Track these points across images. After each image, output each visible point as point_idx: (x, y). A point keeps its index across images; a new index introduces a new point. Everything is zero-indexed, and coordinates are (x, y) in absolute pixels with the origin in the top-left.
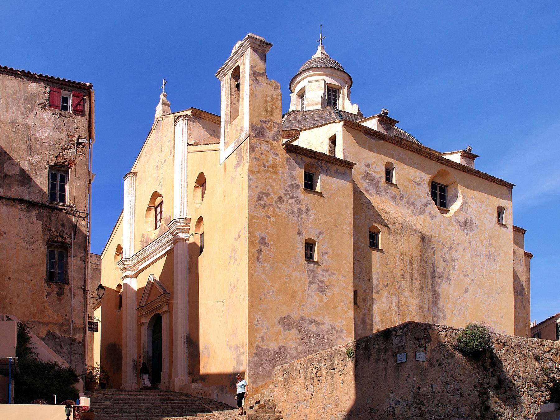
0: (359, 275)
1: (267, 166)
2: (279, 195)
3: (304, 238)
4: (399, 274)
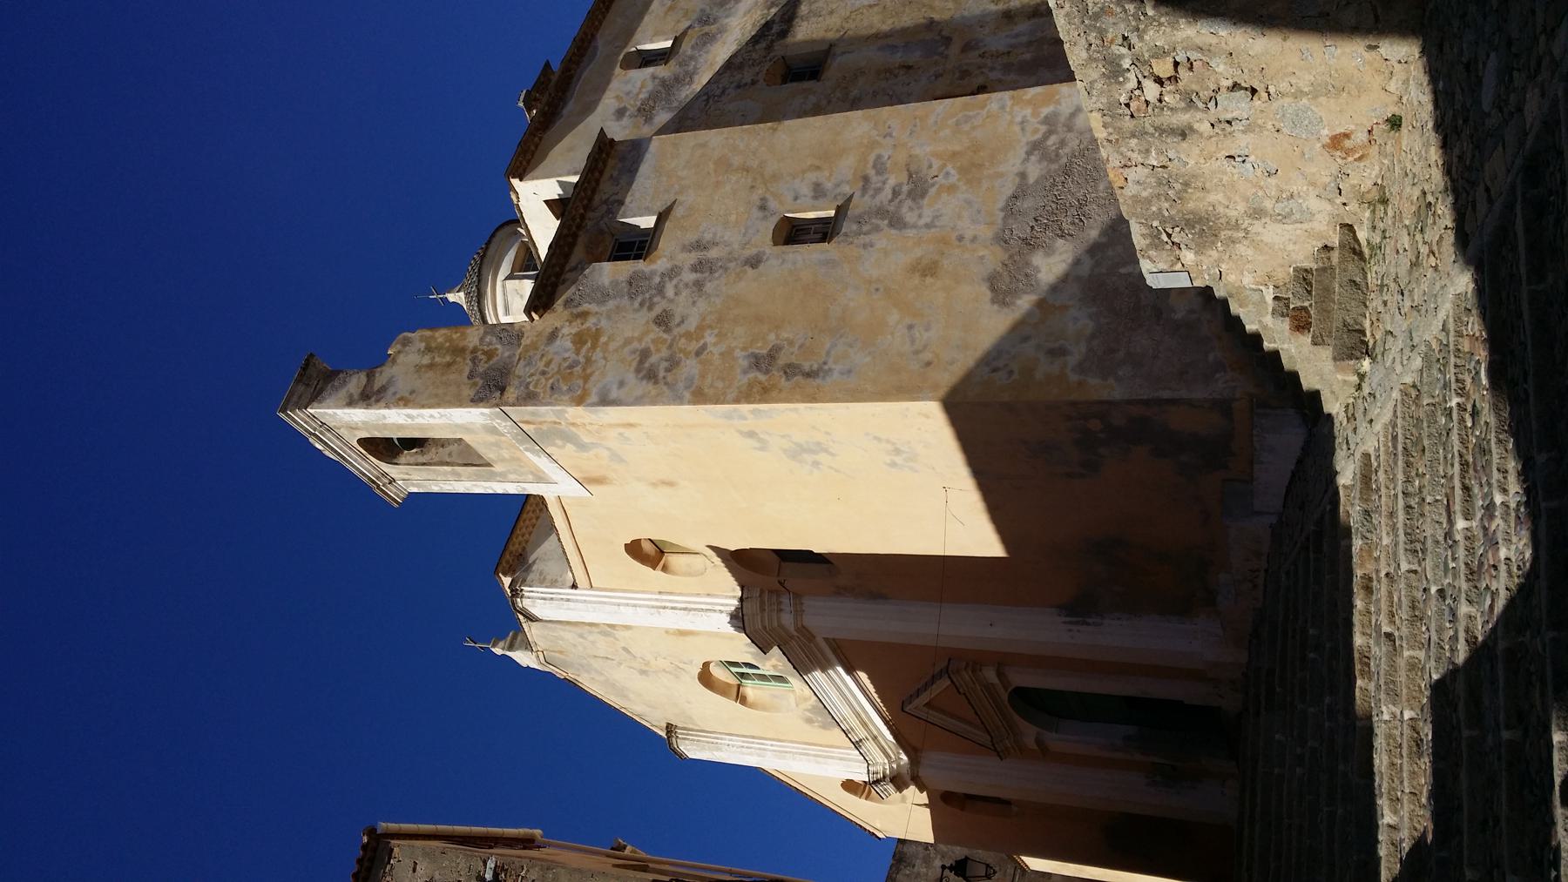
1: (576, 358)
3: (769, 249)
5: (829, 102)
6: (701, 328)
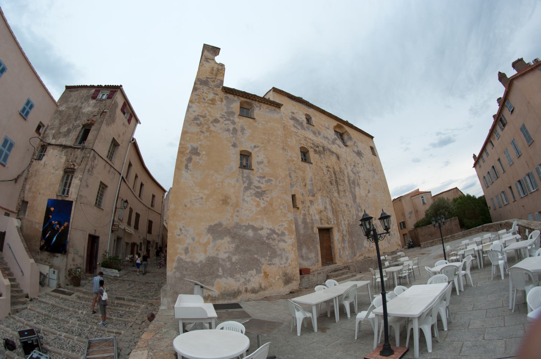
0: (296, 182)
2: (216, 118)
3: (238, 150)
4: (328, 181)
5: (295, 164)
6: (211, 132)
